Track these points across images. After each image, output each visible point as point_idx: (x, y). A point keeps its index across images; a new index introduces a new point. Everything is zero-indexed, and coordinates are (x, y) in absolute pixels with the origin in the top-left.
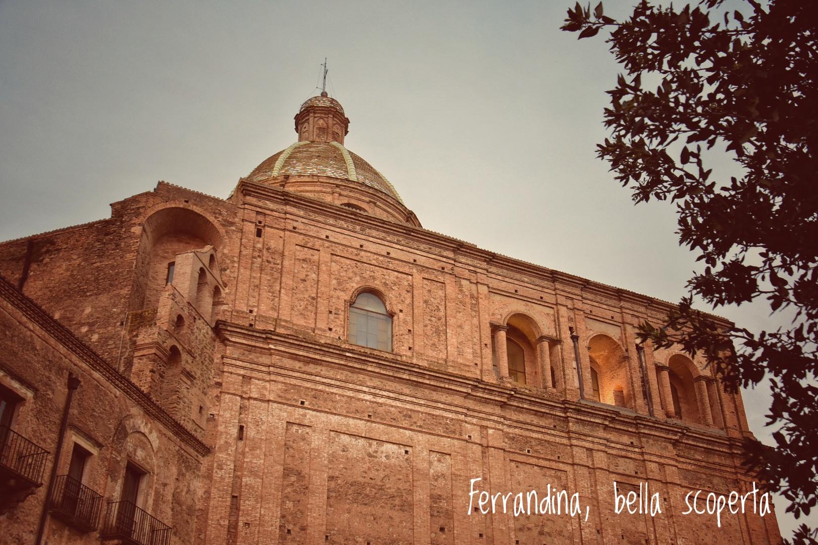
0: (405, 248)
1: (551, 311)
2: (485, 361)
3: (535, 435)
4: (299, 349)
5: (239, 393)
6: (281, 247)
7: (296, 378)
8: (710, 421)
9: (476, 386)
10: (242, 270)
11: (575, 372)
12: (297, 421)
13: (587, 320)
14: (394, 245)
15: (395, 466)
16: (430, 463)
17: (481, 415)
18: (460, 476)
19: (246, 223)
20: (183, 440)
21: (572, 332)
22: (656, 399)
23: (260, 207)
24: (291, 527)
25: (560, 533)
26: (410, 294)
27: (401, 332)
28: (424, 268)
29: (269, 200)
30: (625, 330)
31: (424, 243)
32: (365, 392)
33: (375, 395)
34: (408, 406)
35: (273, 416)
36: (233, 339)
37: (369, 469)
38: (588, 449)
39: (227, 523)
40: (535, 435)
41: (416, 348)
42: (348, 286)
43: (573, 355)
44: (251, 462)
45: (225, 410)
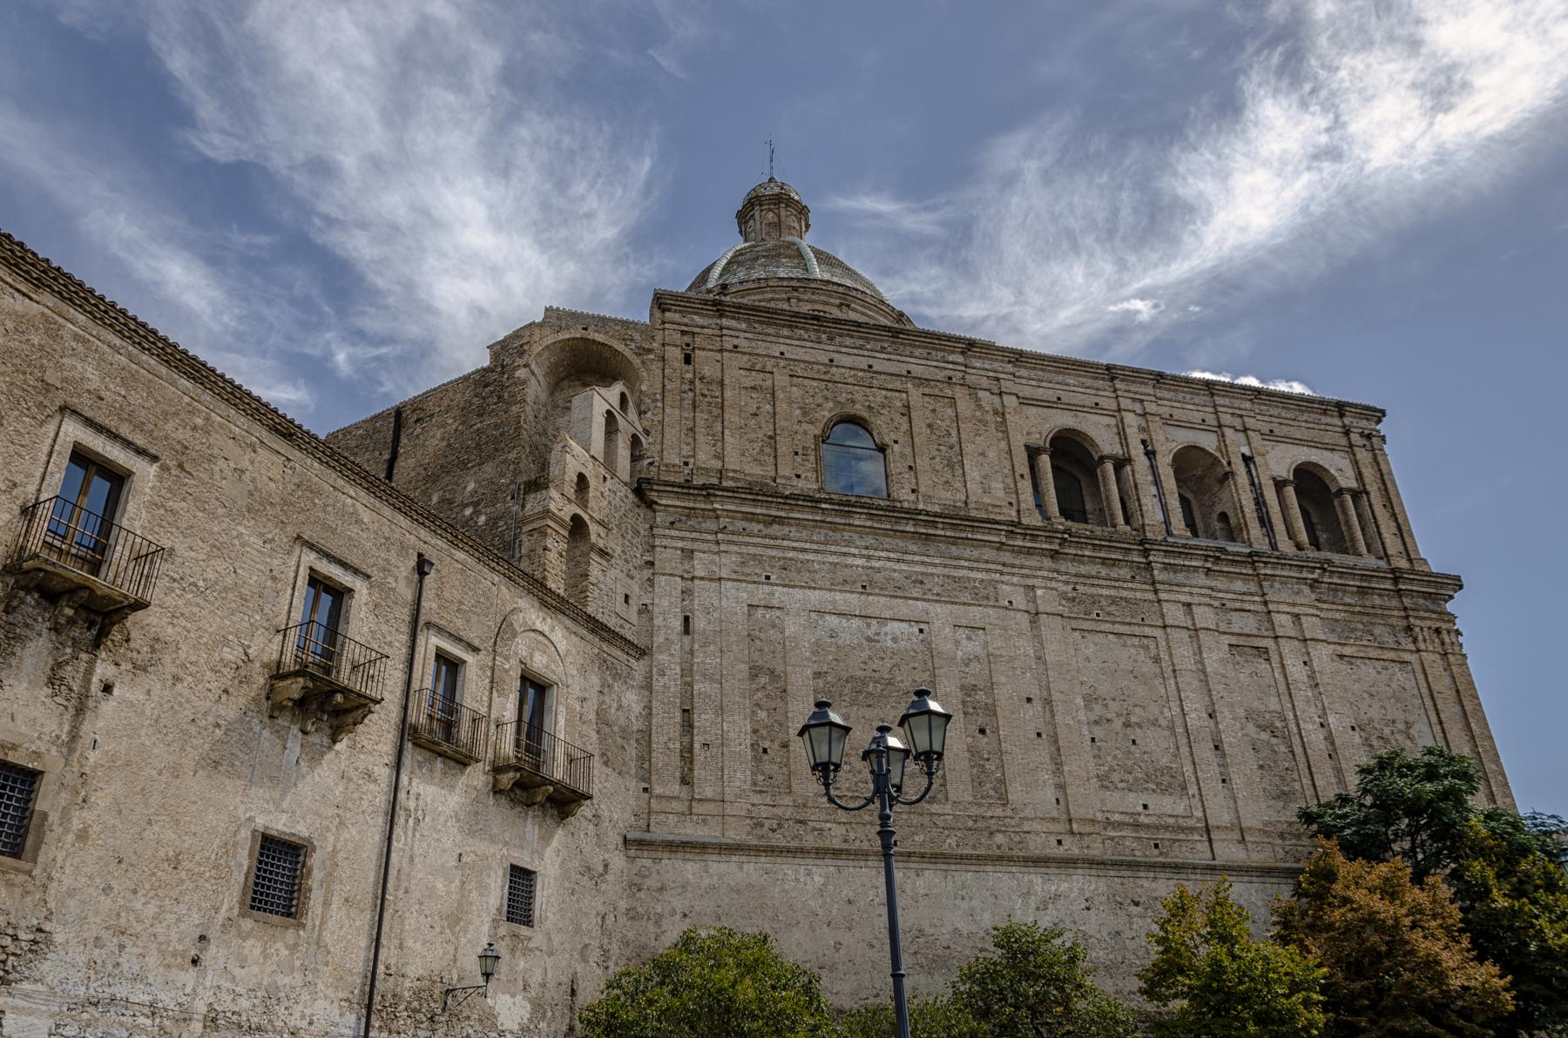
0: (893, 357)
1: (1112, 421)
2: (1022, 497)
3: (1105, 592)
4: (756, 506)
5: (679, 572)
6: (719, 374)
7: (754, 545)
8: (1363, 549)
9: (1012, 532)
10: (668, 410)
11: (1156, 500)
12: (763, 603)
13: (1167, 427)
14: (878, 355)
15: (906, 650)
16: (957, 643)
17: (1024, 571)
18: (1001, 656)
19: (667, 348)
20: (603, 639)
21: (1145, 447)
22: (1279, 526)
23: (686, 325)
24: (767, 744)
25: (1155, 723)
26: (905, 418)
27: (898, 471)
28: (921, 381)
29: (696, 314)
30: (1223, 436)
31: (919, 347)
32: (854, 555)
33: (869, 558)
34: (918, 569)
35: (728, 599)
36: (664, 502)
37: (870, 658)
38: (1184, 604)
39: (678, 745)
40: (1105, 592)
41: (922, 489)
42: (817, 415)
43: (1150, 478)
44: (703, 662)
45: (661, 597)
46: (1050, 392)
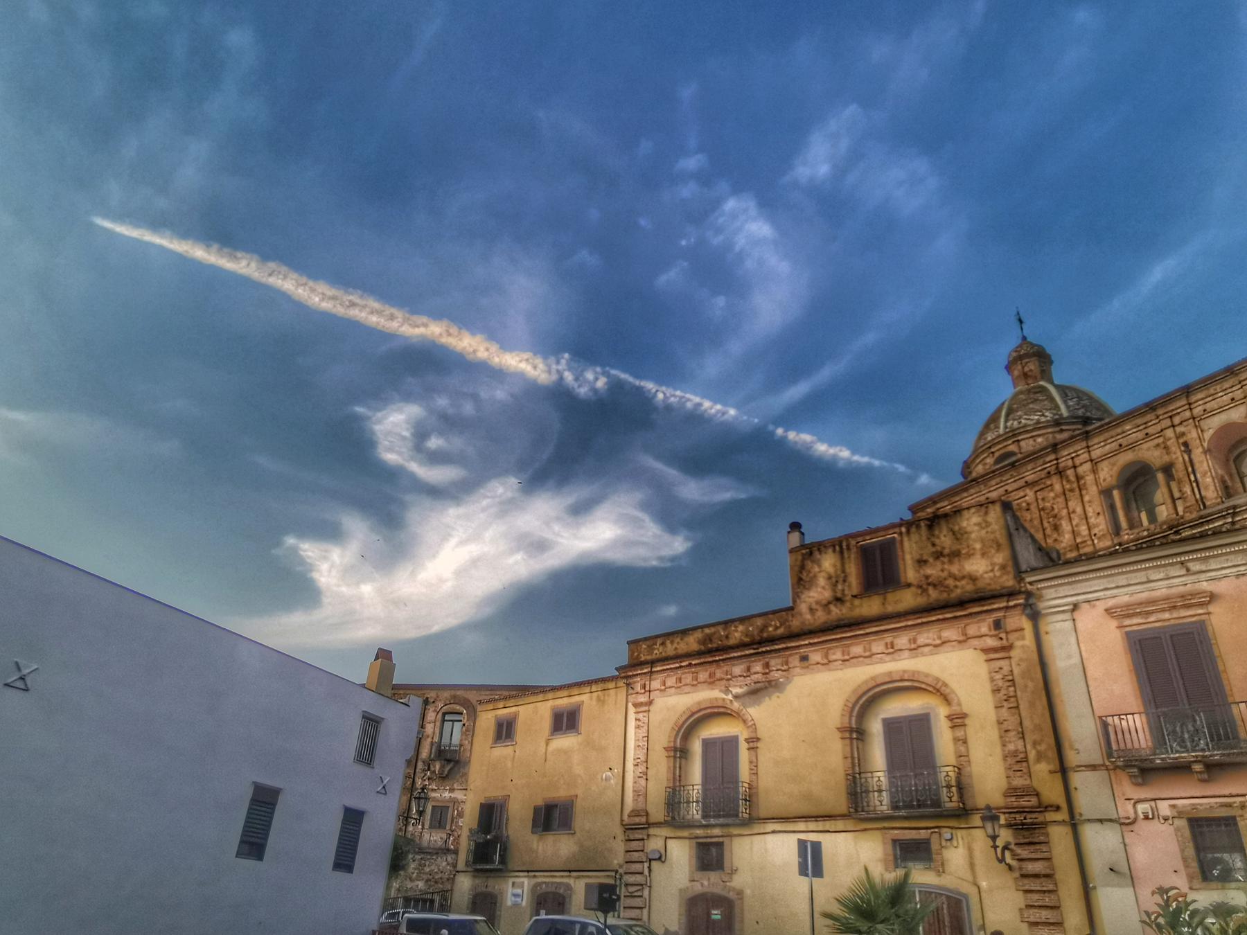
46: (1114, 444)
